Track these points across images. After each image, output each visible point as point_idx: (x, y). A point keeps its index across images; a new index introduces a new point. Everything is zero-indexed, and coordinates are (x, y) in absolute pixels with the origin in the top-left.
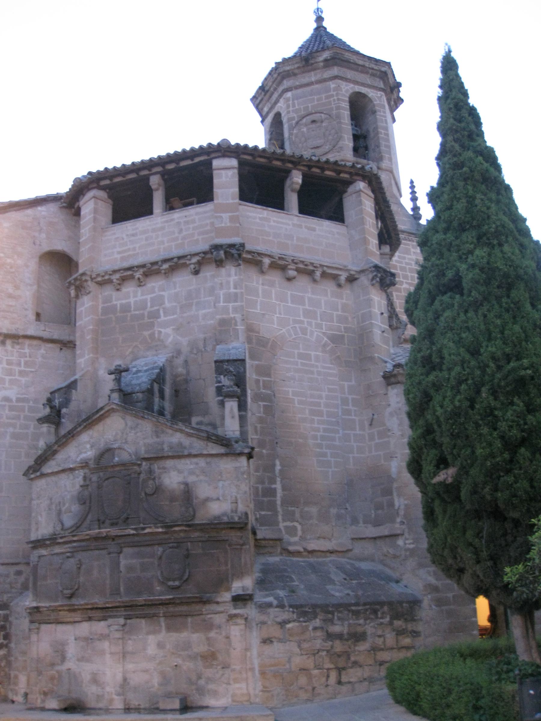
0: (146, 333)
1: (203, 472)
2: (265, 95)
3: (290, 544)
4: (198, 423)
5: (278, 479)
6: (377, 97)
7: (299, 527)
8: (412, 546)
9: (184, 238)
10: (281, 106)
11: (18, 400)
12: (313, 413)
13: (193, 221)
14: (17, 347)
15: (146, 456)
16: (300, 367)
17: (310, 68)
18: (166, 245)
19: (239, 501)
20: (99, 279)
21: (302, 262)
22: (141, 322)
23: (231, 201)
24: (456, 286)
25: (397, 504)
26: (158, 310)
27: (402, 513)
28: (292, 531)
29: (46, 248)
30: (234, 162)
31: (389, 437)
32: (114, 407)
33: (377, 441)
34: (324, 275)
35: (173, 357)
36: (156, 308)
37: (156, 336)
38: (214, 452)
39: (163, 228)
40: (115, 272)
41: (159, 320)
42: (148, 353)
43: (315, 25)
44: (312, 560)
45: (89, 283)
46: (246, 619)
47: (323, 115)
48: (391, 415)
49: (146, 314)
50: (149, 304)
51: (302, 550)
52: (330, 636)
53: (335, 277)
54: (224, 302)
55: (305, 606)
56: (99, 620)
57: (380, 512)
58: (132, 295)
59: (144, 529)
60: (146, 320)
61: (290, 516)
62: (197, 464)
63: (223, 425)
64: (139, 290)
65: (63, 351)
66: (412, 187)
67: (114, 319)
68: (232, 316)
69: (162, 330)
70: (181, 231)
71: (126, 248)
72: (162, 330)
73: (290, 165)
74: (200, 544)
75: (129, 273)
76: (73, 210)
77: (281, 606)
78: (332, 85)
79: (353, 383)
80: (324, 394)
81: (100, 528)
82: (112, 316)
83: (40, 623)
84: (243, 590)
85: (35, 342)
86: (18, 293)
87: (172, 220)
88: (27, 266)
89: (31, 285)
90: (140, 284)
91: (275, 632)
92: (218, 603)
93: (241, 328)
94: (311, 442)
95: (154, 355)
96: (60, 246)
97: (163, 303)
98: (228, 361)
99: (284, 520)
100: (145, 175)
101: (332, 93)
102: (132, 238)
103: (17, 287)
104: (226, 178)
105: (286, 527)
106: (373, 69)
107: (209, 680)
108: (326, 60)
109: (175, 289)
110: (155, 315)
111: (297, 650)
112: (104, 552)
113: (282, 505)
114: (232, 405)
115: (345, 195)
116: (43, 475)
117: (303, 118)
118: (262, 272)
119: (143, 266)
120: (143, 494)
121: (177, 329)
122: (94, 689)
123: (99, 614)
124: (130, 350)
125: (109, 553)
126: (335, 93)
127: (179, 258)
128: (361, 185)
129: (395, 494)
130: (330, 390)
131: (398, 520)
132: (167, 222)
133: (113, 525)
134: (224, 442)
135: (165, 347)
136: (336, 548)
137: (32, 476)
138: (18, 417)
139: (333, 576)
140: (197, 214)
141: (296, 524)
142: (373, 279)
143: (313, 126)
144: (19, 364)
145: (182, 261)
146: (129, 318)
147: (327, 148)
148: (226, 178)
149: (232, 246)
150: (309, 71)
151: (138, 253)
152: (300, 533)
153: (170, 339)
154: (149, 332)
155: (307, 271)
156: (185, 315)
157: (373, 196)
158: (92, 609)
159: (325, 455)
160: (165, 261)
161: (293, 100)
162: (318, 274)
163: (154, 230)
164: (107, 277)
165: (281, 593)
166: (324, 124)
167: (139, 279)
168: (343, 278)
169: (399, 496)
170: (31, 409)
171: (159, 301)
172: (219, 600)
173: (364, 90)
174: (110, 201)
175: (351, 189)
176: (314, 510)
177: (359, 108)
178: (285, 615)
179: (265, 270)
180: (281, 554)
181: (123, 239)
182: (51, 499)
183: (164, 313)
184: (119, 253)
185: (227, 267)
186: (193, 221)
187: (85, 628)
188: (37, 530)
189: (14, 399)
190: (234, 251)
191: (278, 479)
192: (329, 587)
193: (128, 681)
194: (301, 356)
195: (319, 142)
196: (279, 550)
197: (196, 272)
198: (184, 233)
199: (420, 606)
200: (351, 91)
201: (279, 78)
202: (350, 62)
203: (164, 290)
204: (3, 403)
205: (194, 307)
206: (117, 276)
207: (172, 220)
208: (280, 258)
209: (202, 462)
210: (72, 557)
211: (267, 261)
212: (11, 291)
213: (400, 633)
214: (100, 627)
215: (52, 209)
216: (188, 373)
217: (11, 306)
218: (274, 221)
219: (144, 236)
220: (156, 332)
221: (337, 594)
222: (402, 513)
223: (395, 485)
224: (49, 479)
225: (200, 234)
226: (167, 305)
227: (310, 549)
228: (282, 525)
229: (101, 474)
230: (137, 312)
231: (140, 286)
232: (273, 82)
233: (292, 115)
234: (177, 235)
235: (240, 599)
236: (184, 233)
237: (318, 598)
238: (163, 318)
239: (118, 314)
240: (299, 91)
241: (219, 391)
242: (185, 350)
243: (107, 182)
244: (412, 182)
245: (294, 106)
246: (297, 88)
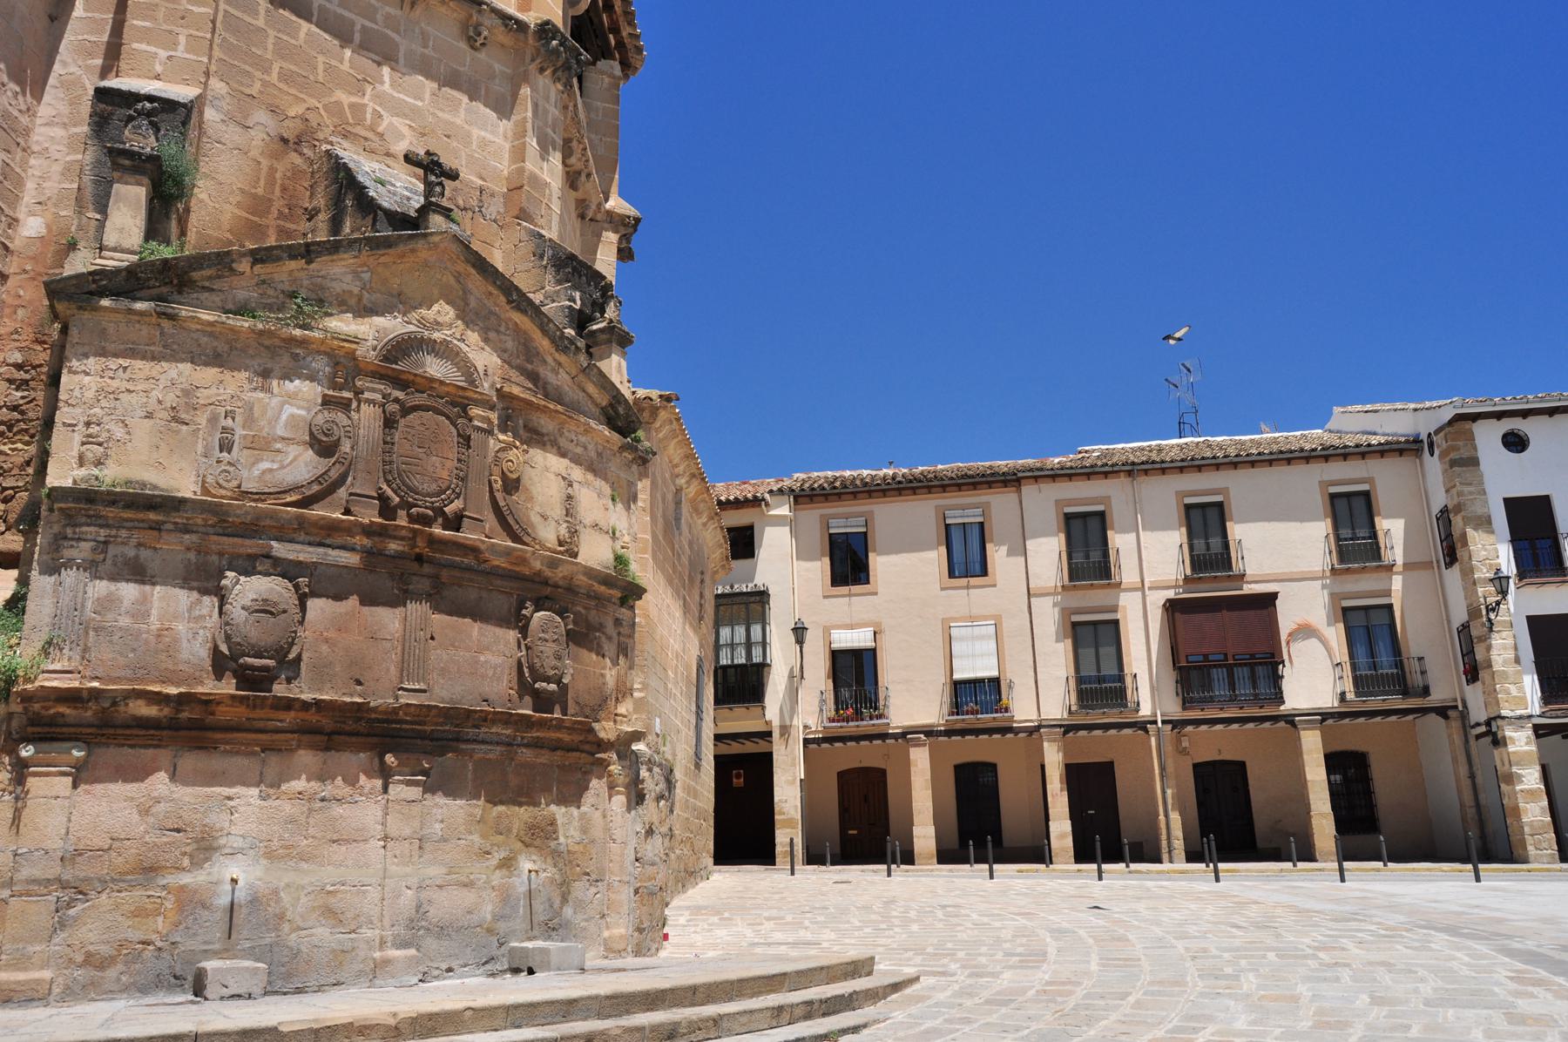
0: (345, 98)
22: (334, 63)
37: (368, 116)
107: (580, 905)
109: (425, 47)
122: (323, 933)
154: (354, 99)
156: (440, 114)
193: (425, 907)
203: (398, 32)
220: (369, 110)
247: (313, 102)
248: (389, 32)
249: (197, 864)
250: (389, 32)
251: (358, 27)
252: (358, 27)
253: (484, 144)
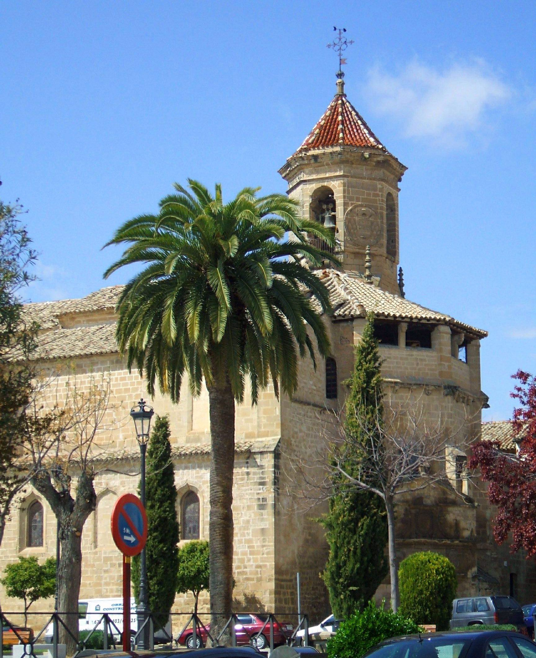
8: (496, 556)
9: (419, 369)
13: (425, 360)
87: (412, 355)
126: (380, 193)
132: (409, 355)
140: (427, 356)
163: (401, 359)
186: (425, 360)
207: (412, 355)
234: (415, 366)
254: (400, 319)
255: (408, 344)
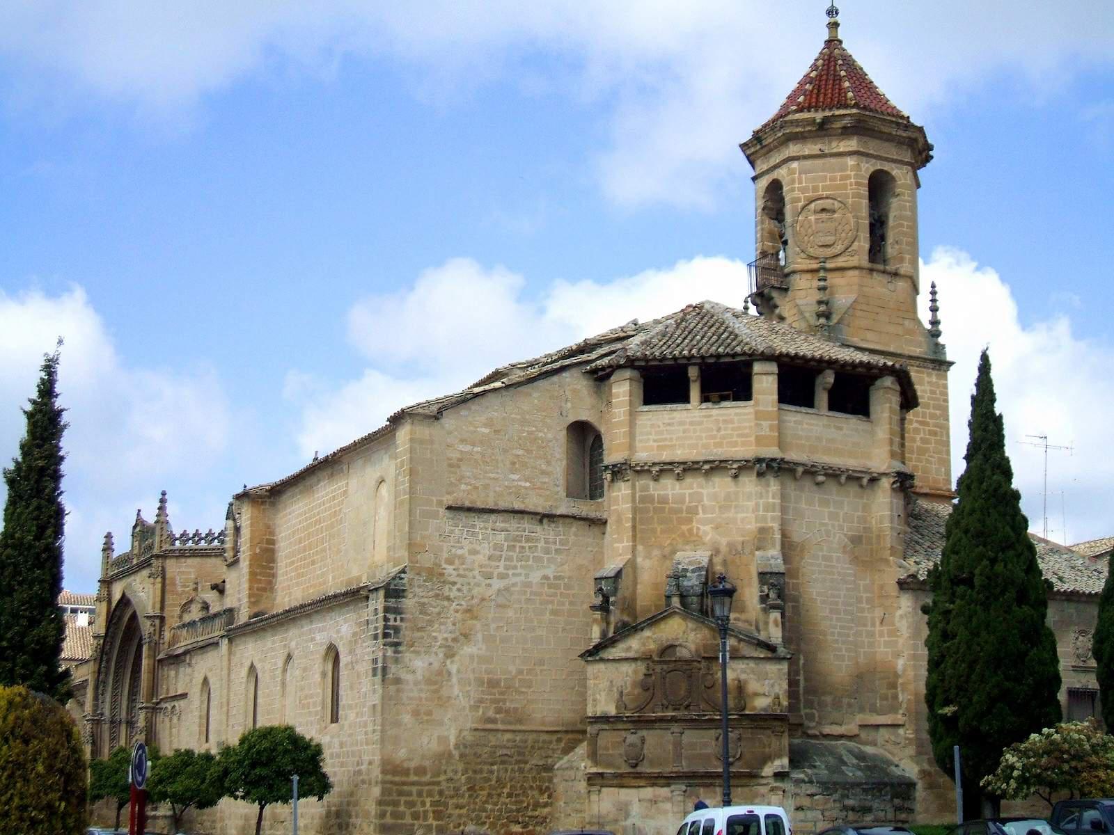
0: (685, 528)
1: (753, 672)
2: (762, 148)
3: (809, 728)
4: (735, 619)
5: (802, 672)
6: (900, 174)
7: (817, 715)
9: (723, 437)
10: (781, 174)
11: (556, 578)
12: (831, 611)
13: (731, 422)
14: (553, 525)
15: (706, 655)
16: (823, 568)
17: (825, 132)
18: (704, 441)
19: (781, 697)
20: (639, 468)
21: (831, 468)
22: (679, 515)
23: (770, 409)
24: (969, 582)
25: (901, 698)
26: (697, 507)
27: (904, 706)
28: (811, 717)
29: (572, 419)
30: (773, 367)
31: (898, 636)
32: (677, 610)
33: (886, 639)
34: (849, 478)
35: (712, 555)
36: (694, 504)
37: (695, 531)
38: (762, 656)
39: (700, 423)
40: (654, 464)
41: (698, 516)
42: (687, 547)
43: (825, 35)
44: (826, 742)
45: (629, 471)
46: (784, 791)
47: (836, 203)
48: (901, 616)
49: (684, 508)
50: (687, 499)
51: (818, 733)
52: (845, 808)
53: (859, 479)
54: (764, 511)
55: (829, 783)
56: (662, 787)
57: (885, 702)
58: (669, 488)
59: (706, 715)
60: (684, 515)
61: (810, 704)
62: (748, 664)
63: (766, 629)
64: (677, 485)
65: (591, 528)
66: (933, 293)
67: (652, 509)
68: (771, 525)
69: (702, 527)
70: (719, 430)
71: (663, 437)
72: (702, 527)
73: (824, 365)
74: (750, 730)
75: (670, 467)
76: (596, 376)
77: (811, 782)
78: (851, 161)
79: (868, 582)
80: (842, 593)
81: (663, 712)
82: (649, 505)
83: (602, 786)
84: (782, 768)
85: (568, 520)
86: (550, 469)
88: (557, 440)
89: (561, 460)
90: (679, 478)
91: (806, 802)
92: (763, 777)
93: (778, 536)
94: (829, 638)
95: (692, 550)
96: (584, 416)
97: (703, 501)
98: (771, 573)
99: (805, 708)
100: (683, 364)
101: (849, 173)
102: (668, 428)
103: (549, 463)
104: (765, 382)
105: (806, 714)
106: (900, 136)
108: (844, 128)
109: (714, 488)
110: (693, 511)
111: (821, 817)
112: (669, 732)
113: (804, 693)
114: (775, 615)
115: (871, 388)
116: (602, 660)
117: (811, 202)
118: (795, 479)
119: (684, 463)
120: (703, 687)
121: (717, 528)
123: (662, 781)
124: (668, 542)
125: (673, 733)
127: (721, 461)
128: (888, 381)
129: (899, 689)
130: (848, 590)
131: (901, 712)
132: (705, 416)
133: (675, 710)
134: (771, 648)
135: (704, 544)
136: (845, 733)
137: (589, 659)
138: (555, 595)
139: (845, 758)
140: (736, 414)
141: (814, 711)
142: (894, 483)
143: (824, 215)
144: (555, 543)
145: (722, 465)
146: (667, 510)
147: (839, 248)
148: (765, 382)
149: (773, 460)
150: (825, 136)
151: (675, 445)
152: (817, 719)
153: (708, 538)
155: (833, 474)
156: (723, 516)
157: (898, 388)
158: (656, 778)
159: (840, 650)
160: (706, 462)
161: (800, 174)
162: (843, 478)
163: (691, 423)
164: (646, 468)
165: (809, 771)
166: (836, 215)
167: (678, 474)
168: (865, 481)
169: (903, 691)
170: (567, 587)
171: (698, 497)
172: (763, 774)
173: (886, 167)
174: (642, 380)
175: (878, 383)
176: (829, 699)
177: (879, 187)
178: (812, 789)
179: (798, 478)
180: (801, 737)
181: (659, 427)
182: (611, 682)
183: (703, 510)
184: (655, 441)
185: (767, 477)
186: (731, 422)
187: (648, 792)
188: (595, 706)
189: (552, 577)
190: (775, 465)
191: (802, 672)
192: (843, 768)
194: (826, 558)
195: (829, 239)
196: (800, 733)
197: (736, 477)
198: (723, 432)
199: (915, 788)
200: (872, 169)
201: (783, 138)
202: (874, 130)
204: (543, 581)
205: (733, 510)
206: (657, 468)
208: (812, 466)
209: (752, 664)
210: (635, 733)
211: (800, 469)
212: (544, 467)
213: (898, 809)
214: (664, 791)
215: (575, 375)
216: (727, 571)
217: (545, 483)
218: (807, 424)
219: (681, 428)
221: (851, 774)
222: (904, 706)
223: (900, 681)
224: (609, 665)
225: (739, 436)
226: (706, 502)
227: (825, 733)
228: (803, 712)
229: (665, 667)
230: (673, 505)
231: (678, 480)
232: (774, 140)
233: (797, 194)
234: (715, 433)
235: (780, 776)
236: (723, 432)
237: (836, 778)
238: (701, 515)
239: (656, 505)
240: (809, 163)
241: (764, 599)
242: (724, 549)
243: (643, 364)
244: (933, 286)
245: (800, 183)
246: (805, 157)
247: (674, 536)
248: (699, 490)
249: (626, 819)
250: (699, 490)
251: (687, 495)
252: (687, 495)
253: (743, 520)
254: (685, 361)
255: (705, 399)
